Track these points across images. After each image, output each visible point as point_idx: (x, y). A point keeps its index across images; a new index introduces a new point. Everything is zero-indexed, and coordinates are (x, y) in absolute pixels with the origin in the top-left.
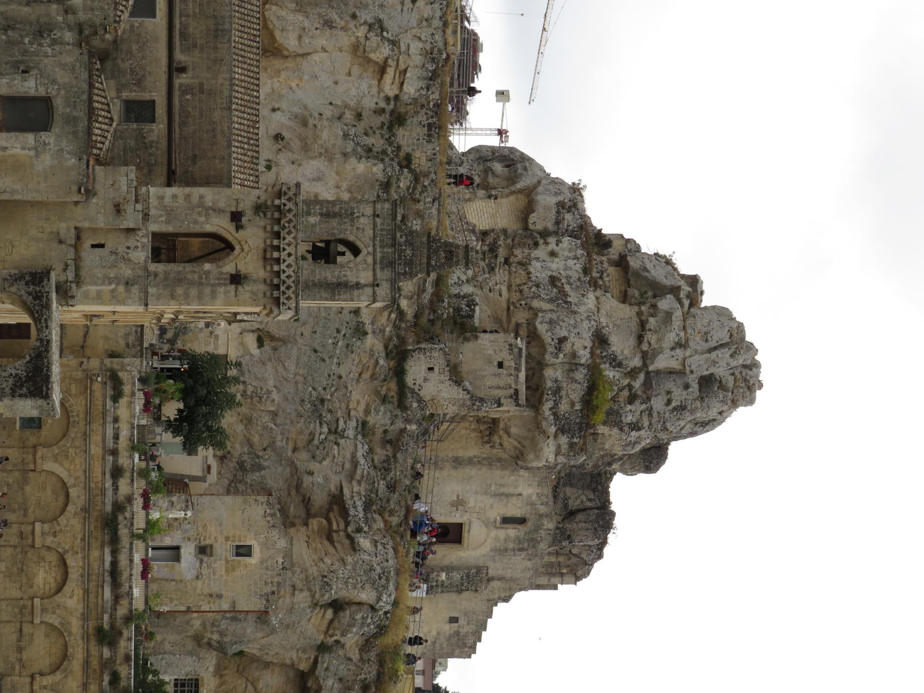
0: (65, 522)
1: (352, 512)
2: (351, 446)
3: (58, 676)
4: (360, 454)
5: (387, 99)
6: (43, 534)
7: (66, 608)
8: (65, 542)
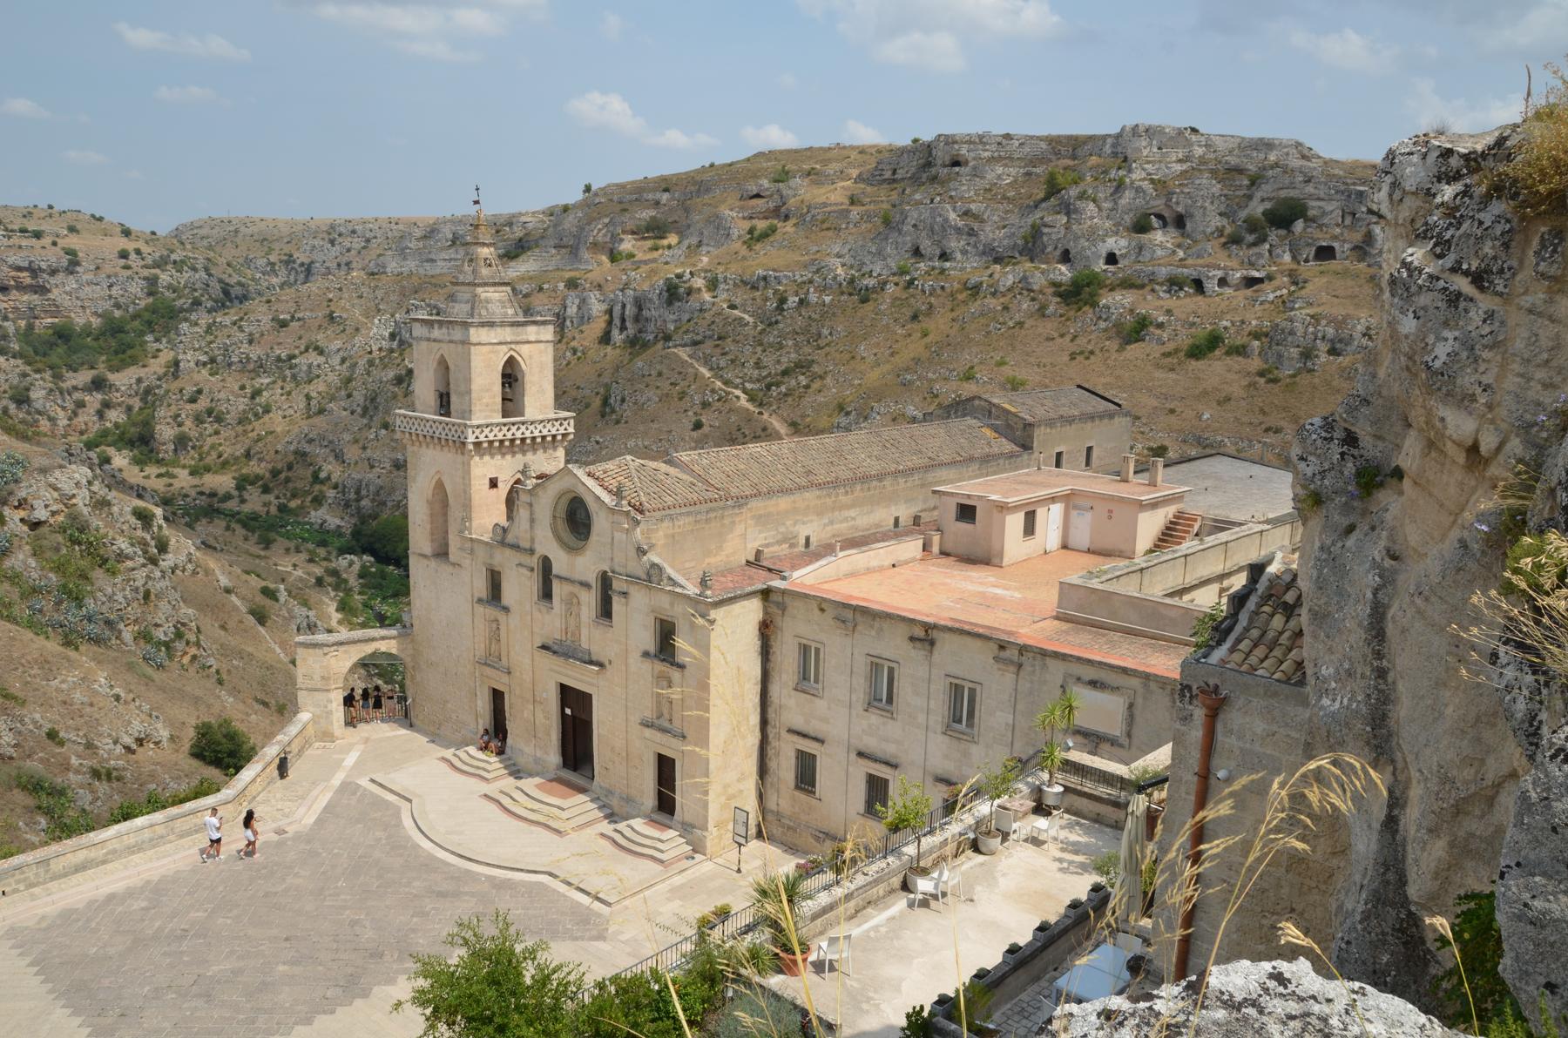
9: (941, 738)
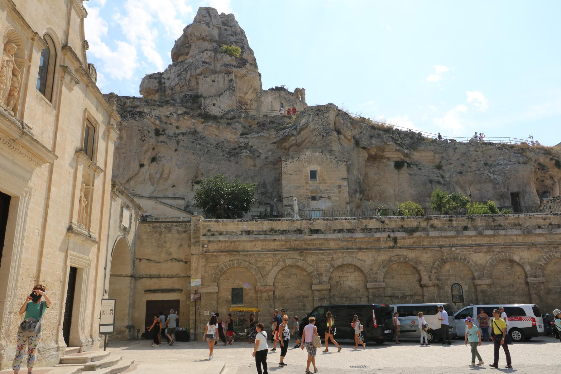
0: (311, 267)
1: (286, 134)
2: (253, 140)
3: (420, 268)
4: (256, 136)
6: (320, 283)
7: (372, 264)
8: (323, 266)
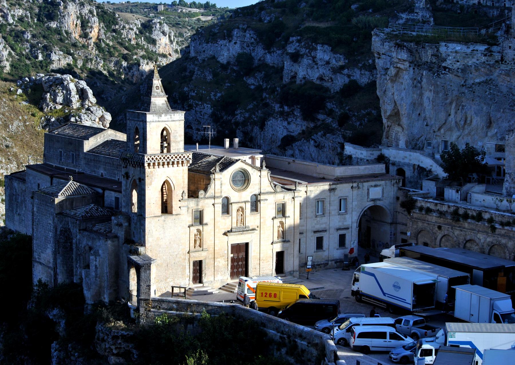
5: (410, 66)
7: (484, 243)
9: (338, 216)
